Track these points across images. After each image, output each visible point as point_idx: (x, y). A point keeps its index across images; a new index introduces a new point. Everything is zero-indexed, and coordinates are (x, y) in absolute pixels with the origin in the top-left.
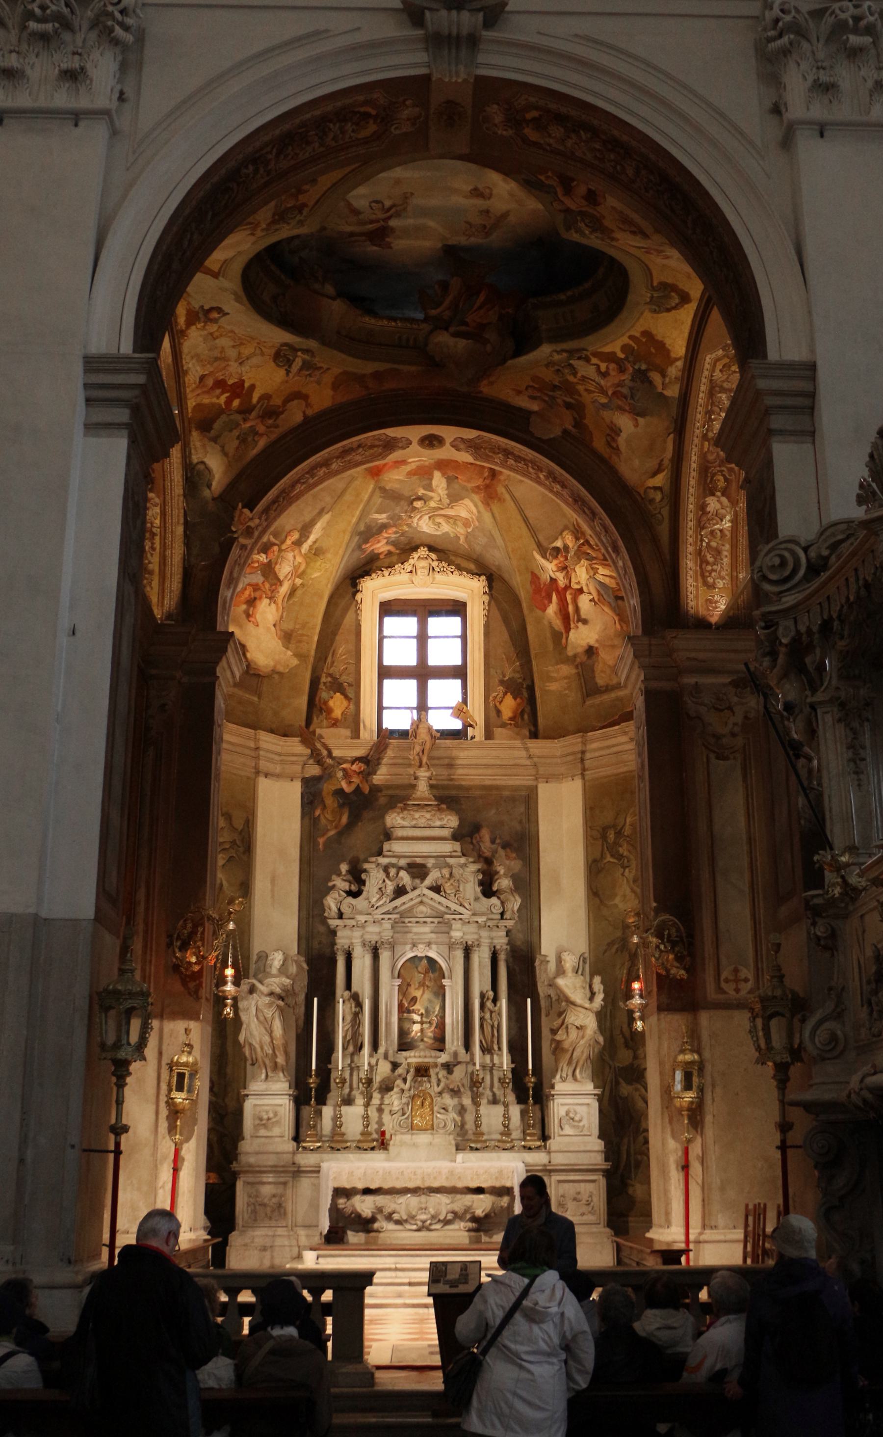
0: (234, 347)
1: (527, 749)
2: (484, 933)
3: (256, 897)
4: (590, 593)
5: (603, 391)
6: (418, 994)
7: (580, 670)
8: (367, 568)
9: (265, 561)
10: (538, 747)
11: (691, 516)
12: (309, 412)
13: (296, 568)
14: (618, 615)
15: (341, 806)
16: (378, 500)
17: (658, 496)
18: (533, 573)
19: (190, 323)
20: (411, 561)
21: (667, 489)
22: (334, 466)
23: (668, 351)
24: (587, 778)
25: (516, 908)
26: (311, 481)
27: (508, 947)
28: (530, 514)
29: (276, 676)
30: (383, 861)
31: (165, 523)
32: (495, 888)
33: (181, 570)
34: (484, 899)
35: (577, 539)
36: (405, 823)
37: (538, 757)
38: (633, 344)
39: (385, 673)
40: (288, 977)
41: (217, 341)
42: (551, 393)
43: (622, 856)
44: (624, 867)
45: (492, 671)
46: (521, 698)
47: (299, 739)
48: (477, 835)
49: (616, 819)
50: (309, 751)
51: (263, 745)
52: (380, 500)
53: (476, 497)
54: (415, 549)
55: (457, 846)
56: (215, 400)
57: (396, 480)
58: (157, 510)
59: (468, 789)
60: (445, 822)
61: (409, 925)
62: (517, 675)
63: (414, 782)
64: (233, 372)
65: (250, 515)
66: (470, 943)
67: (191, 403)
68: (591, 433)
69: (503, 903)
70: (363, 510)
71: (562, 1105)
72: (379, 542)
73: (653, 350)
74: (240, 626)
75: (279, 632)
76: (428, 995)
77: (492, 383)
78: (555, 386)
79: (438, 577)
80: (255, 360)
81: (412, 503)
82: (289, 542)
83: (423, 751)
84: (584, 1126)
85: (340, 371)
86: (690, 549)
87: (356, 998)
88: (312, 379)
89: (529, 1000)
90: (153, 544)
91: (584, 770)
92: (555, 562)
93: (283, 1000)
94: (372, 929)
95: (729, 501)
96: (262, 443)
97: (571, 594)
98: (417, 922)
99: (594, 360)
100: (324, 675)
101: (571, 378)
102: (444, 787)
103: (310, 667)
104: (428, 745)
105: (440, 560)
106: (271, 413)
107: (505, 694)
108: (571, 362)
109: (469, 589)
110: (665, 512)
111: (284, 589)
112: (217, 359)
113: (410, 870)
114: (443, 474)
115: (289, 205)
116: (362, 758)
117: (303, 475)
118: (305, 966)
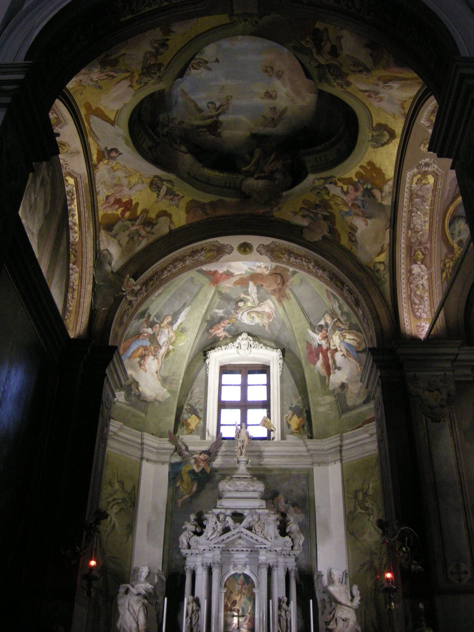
0: (126, 177)
1: (306, 446)
2: (281, 559)
3: (137, 534)
4: (341, 351)
5: (346, 204)
6: (237, 598)
7: (337, 398)
8: (213, 346)
9: (151, 333)
10: (313, 444)
11: (403, 276)
12: (173, 227)
13: (170, 339)
14: (359, 362)
15: (193, 480)
16: (217, 300)
17: (382, 267)
18: (308, 342)
19: (100, 160)
20: (238, 341)
21: (387, 262)
22: (188, 262)
23: (384, 175)
24: (343, 462)
25: (301, 543)
26: (174, 271)
27: (297, 569)
28: (305, 305)
29: (157, 403)
30: (217, 511)
31: (81, 283)
32: (287, 531)
33: (89, 310)
34: (280, 538)
35: (333, 318)
36: (231, 488)
37: (314, 450)
38: (363, 172)
39: (222, 405)
40: (151, 584)
41: (116, 173)
42: (314, 211)
44: (370, 515)
45: (285, 402)
46: (303, 417)
47: (167, 439)
48: (276, 498)
50: (174, 447)
51: (145, 441)
52: (219, 300)
53: (274, 298)
54: (240, 334)
55: (263, 503)
56: (115, 212)
58: (77, 275)
59: (270, 470)
60: (255, 488)
61: (232, 552)
62: (300, 405)
63: (237, 465)
64: (126, 195)
65: (135, 283)
66: (271, 564)
67: (101, 213)
68: (339, 235)
69: (292, 540)
70: (209, 306)
72: (219, 329)
73: (375, 175)
74: (136, 371)
75: (159, 377)
76: (244, 599)
77: (279, 209)
78: (317, 205)
79: (253, 350)
80: (139, 186)
81: (237, 303)
82: (165, 322)
85: (190, 199)
86: (404, 296)
87: (197, 601)
88: (174, 203)
89: (311, 601)
90: (73, 295)
91: (341, 457)
92: (320, 334)
93: (147, 600)
94: (209, 555)
95: (426, 267)
96: (144, 243)
98: (237, 551)
99: (340, 184)
100: (186, 405)
101: (326, 197)
102: (256, 469)
103: (177, 399)
104: (246, 443)
105: (254, 341)
106: (149, 223)
107: (293, 415)
108: (326, 185)
109: (271, 357)
110: (387, 276)
111: (163, 351)
112: (116, 185)
113: (234, 517)
114: (255, 283)
115: (152, 63)
117: (169, 265)
118: (164, 578)
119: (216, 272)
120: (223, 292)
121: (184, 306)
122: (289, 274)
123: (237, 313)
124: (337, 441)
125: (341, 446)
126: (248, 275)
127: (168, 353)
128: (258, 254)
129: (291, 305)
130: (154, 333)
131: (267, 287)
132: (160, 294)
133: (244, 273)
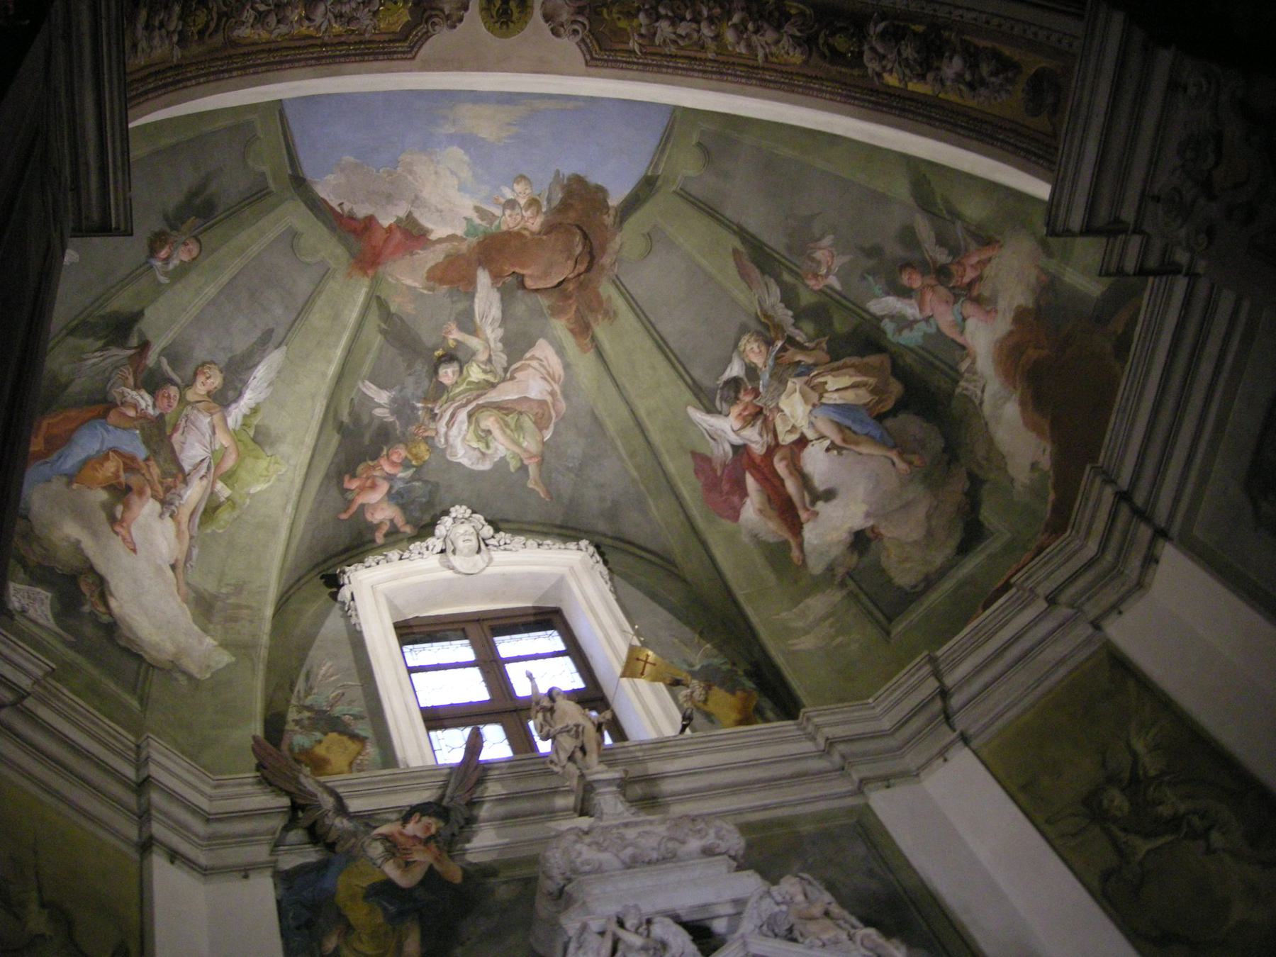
4: (822, 437)
7: (851, 585)
9: (151, 411)
13: (217, 456)
14: (894, 447)
15: (396, 919)
18: (695, 455)
20: (440, 530)
28: (666, 328)
35: (769, 343)
50: (285, 801)
57: (409, 288)
60: (710, 839)
62: (717, 661)
70: (349, 351)
72: (373, 487)
74: (95, 535)
75: (184, 588)
79: (498, 556)
81: (436, 372)
82: (200, 389)
83: (583, 749)
92: (735, 410)
97: (782, 459)
114: (496, 276)
116: (429, 803)
119: (370, 221)
120: (393, 309)
121: (266, 341)
122: (609, 220)
123: (434, 417)
124: (922, 681)
125: (944, 694)
126: (473, 241)
127: (211, 509)
128: (546, 28)
129: (622, 335)
130: (162, 416)
131: (540, 278)
132: (182, 272)
133: (460, 233)
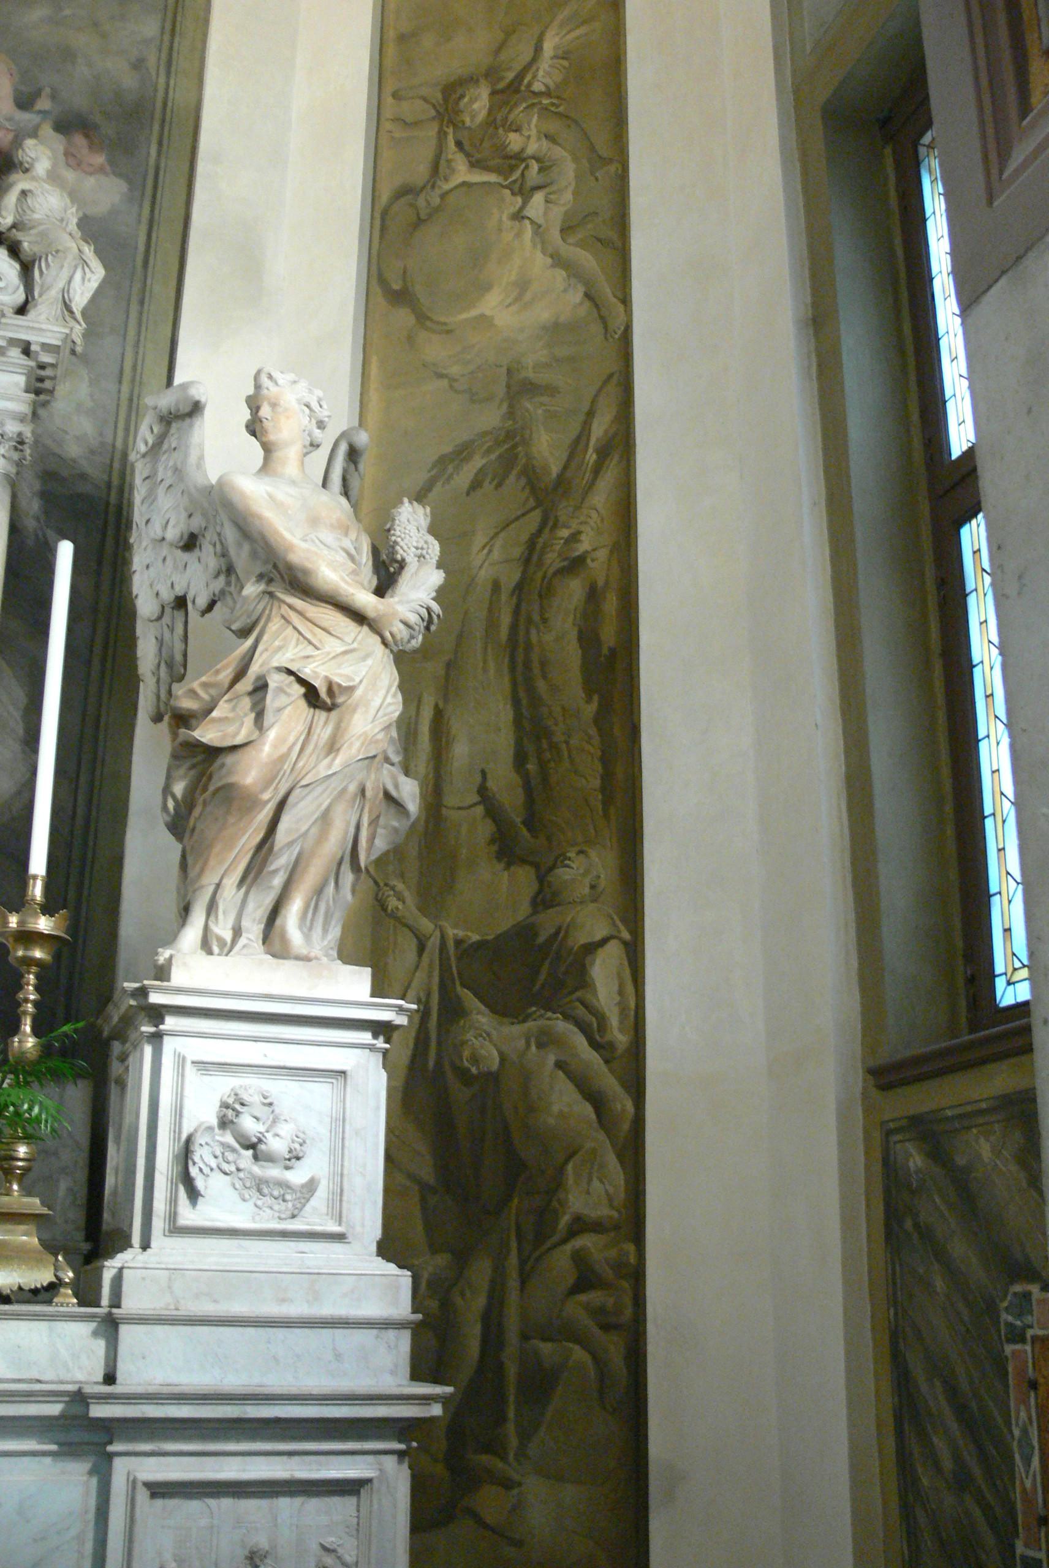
43: (519, 158)
49: (498, 51)
71: (203, 1066)
84: (311, 1186)
